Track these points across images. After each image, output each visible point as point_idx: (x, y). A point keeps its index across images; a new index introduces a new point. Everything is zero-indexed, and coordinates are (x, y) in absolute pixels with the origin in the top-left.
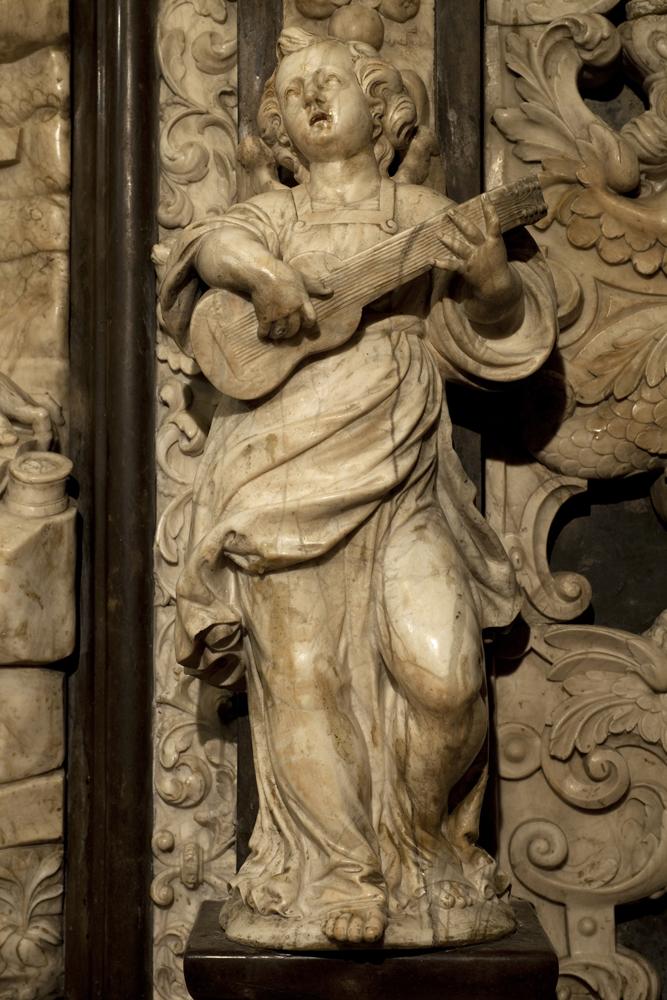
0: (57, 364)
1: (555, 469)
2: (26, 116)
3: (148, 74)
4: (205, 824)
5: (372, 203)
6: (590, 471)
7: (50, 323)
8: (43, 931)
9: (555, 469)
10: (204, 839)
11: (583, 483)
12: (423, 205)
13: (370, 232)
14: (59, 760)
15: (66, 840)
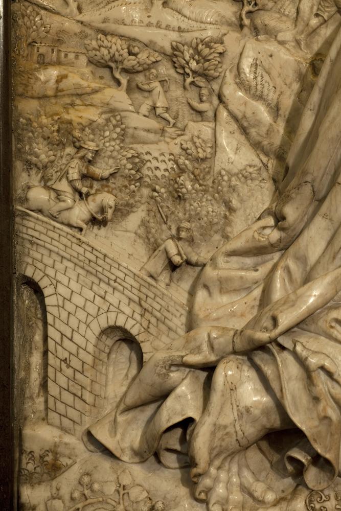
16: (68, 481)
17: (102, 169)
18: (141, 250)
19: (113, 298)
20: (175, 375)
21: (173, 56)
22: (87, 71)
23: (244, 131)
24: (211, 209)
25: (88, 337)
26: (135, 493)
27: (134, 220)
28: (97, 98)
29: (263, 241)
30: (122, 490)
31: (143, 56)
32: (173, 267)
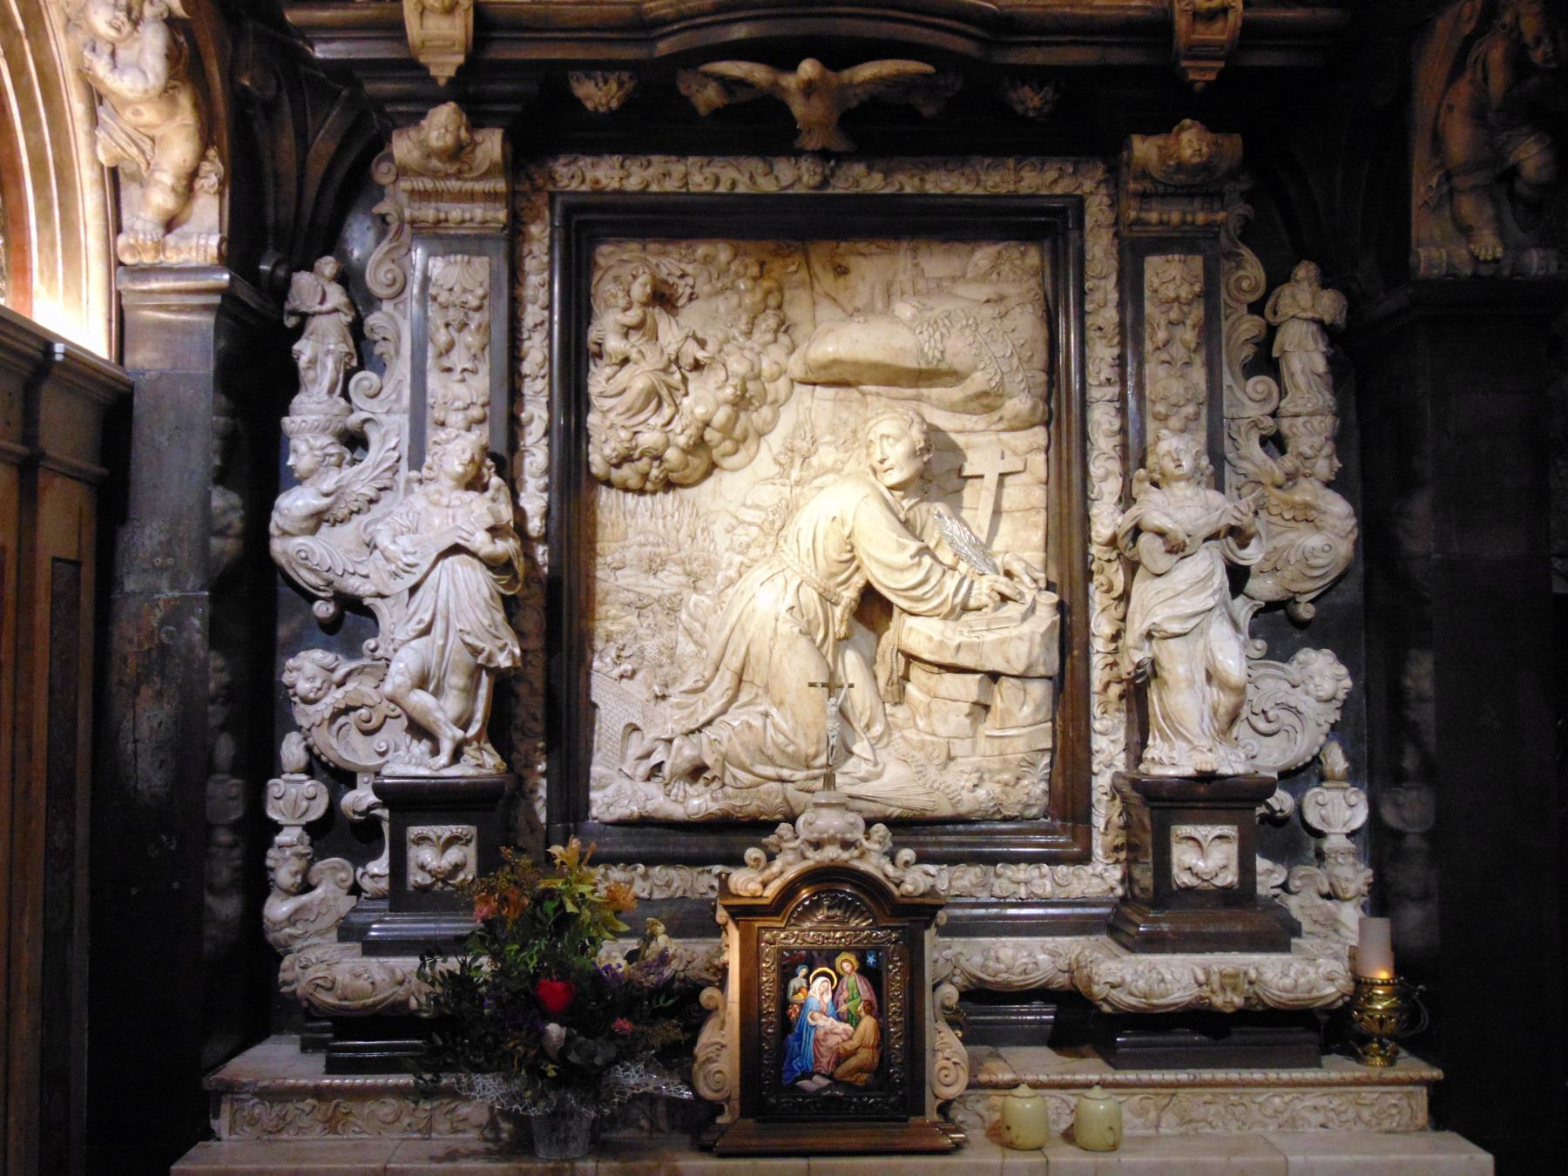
0: (1042, 555)
1: (1252, 598)
2: (1027, 453)
3: (1084, 437)
4: (1113, 742)
5: (1197, 498)
6: (1267, 599)
7: (1037, 537)
8: (1044, 786)
9: (1252, 598)
10: (1112, 747)
11: (1263, 604)
12: (1214, 496)
13: (1199, 510)
14: (1050, 716)
15: (1053, 751)
16: (610, 791)
17: (625, 653)
18: (644, 689)
19: (631, 711)
20: (657, 743)
21: (658, 600)
22: (619, 607)
23: (690, 635)
24: (676, 671)
25: (619, 728)
26: (640, 793)
27: (639, 676)
28: (624, 620)
29: (695, 686)
30: (635, 792)
31: (645, 601)
32: (657, 697)
